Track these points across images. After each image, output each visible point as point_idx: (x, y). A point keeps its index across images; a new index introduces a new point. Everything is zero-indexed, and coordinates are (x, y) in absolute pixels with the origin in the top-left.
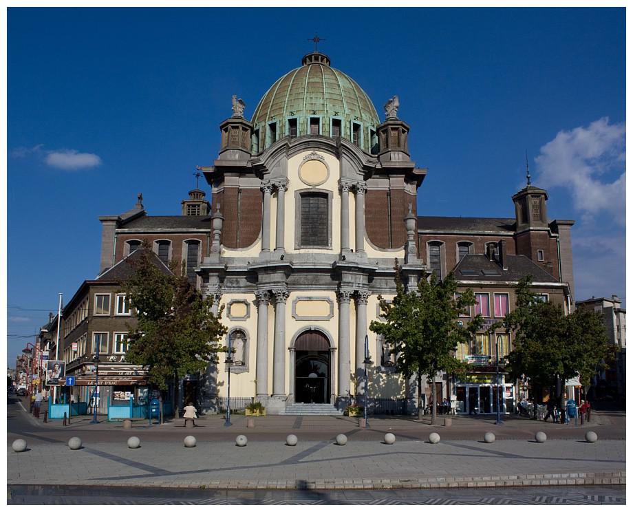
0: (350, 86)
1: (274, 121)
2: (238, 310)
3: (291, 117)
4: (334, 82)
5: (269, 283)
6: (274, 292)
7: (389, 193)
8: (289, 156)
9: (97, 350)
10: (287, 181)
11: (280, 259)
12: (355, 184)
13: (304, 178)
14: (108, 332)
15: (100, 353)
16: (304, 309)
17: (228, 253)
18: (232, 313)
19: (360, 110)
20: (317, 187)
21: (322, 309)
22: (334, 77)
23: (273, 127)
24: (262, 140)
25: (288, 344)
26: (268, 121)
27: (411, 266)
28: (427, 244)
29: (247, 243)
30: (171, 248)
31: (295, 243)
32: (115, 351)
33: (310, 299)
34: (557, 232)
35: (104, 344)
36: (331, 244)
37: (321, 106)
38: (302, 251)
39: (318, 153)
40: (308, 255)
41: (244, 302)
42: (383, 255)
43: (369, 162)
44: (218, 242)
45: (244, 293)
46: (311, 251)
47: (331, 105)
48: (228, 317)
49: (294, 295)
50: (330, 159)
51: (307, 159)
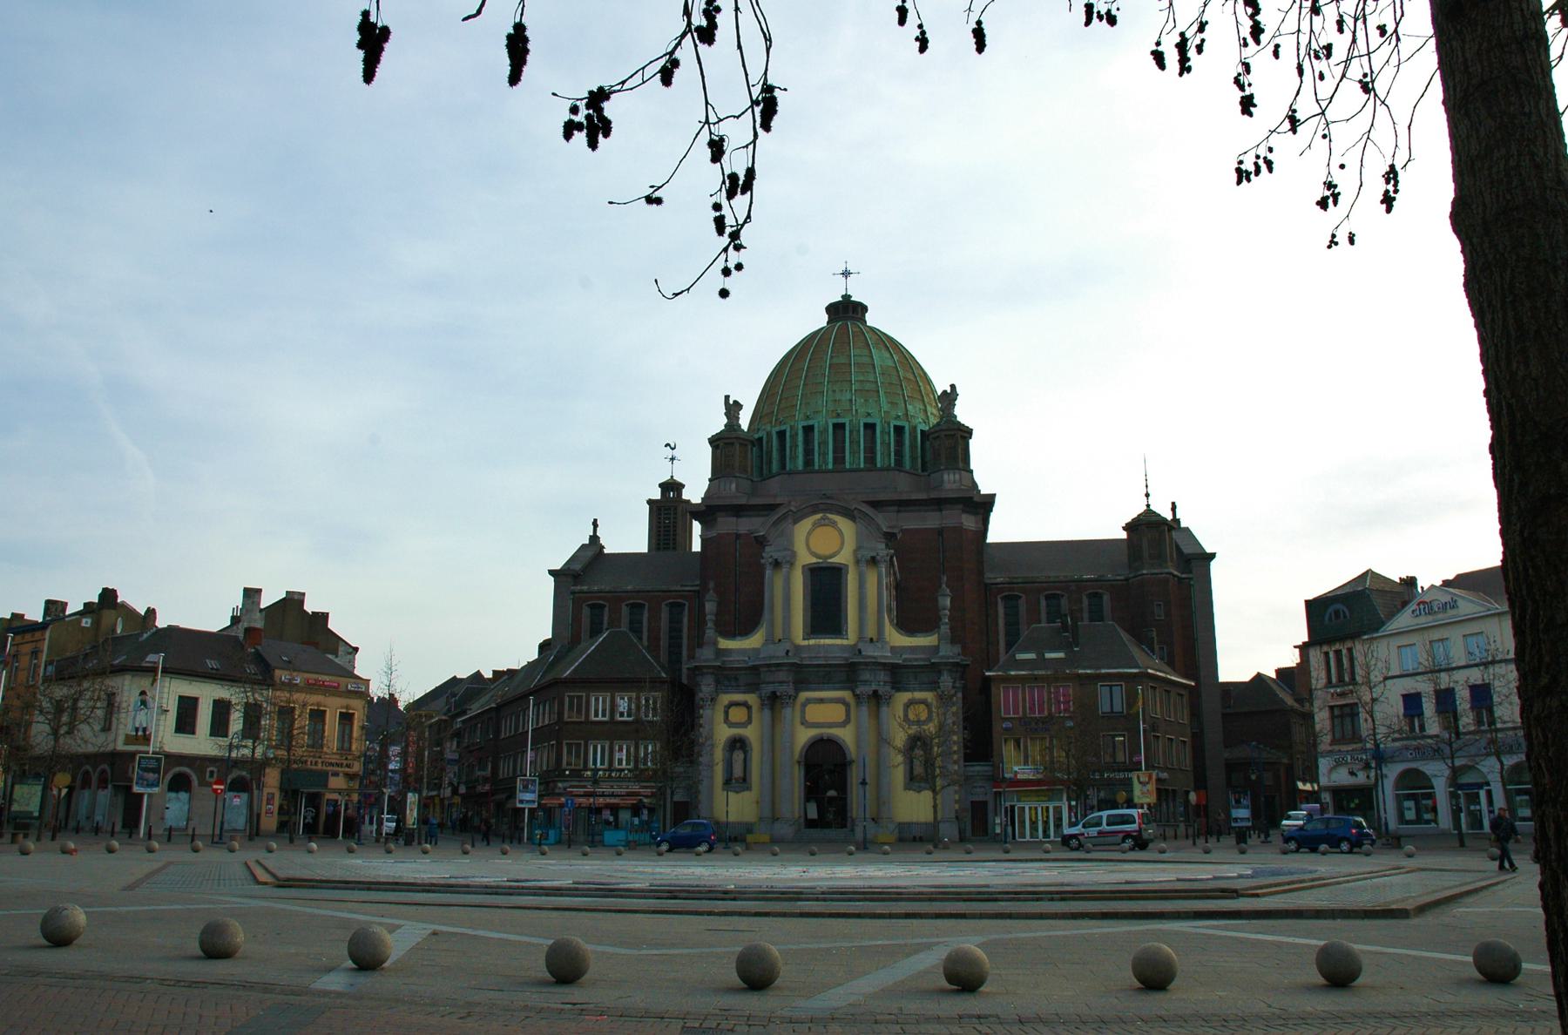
0: (890, 363)
1: (783, 428)
2: (737, 714)
3: (805, 424)
4: (867, 360)
5: (773, 683)
6: (778, 694)
7: (940, 532)
8: (796, 521)
9: (569, 764)
10: (794, 555)
11: (784, 654)
12: (874, 554)
13: (813, 550)
14: (582, 742)
15: (573, 767)
16: (815, 713)
17: (724, 644)
18: (730, 718)
19: (905, 401)
20: (830, 561)
21: (837, 712)
22: (866, 352)
23: (781, 434)
24: (767, 452)
25: (797, 756)
26: (775, 426)
27: (942, 657)
28: (999, 600)
29: (746, 630)
30: (646, 615)
31: (804, 632)
32: (591, 765)
33: (821, 701)
34: (1191, 572)
35: (578, 756)
36: (847, 631)
37: (848, 404)
38: (812, 642)
39: (830, 516)
40: (819, 646)
41: (745, 704)
42: (911, 643)
43: (890, 527)
44: (713, 631)
45: (744, 693)
46: (822, 641)
47: (862, 400)
48: (725, 722)
49: (804, 695)
50: (844, 524)
51: (816, 525)
